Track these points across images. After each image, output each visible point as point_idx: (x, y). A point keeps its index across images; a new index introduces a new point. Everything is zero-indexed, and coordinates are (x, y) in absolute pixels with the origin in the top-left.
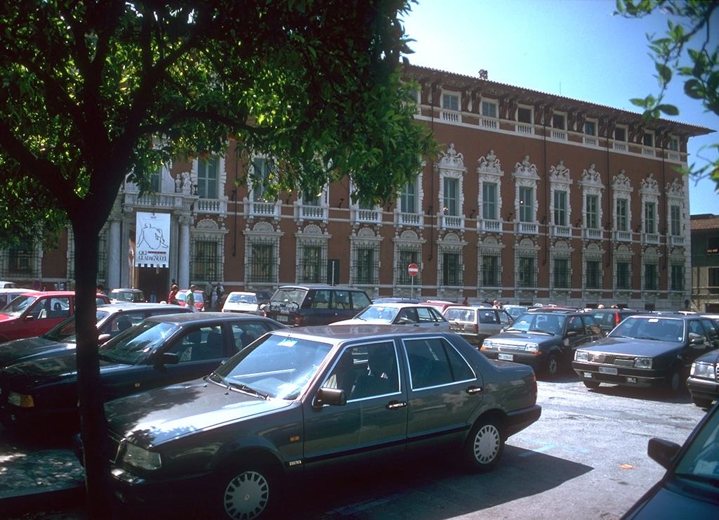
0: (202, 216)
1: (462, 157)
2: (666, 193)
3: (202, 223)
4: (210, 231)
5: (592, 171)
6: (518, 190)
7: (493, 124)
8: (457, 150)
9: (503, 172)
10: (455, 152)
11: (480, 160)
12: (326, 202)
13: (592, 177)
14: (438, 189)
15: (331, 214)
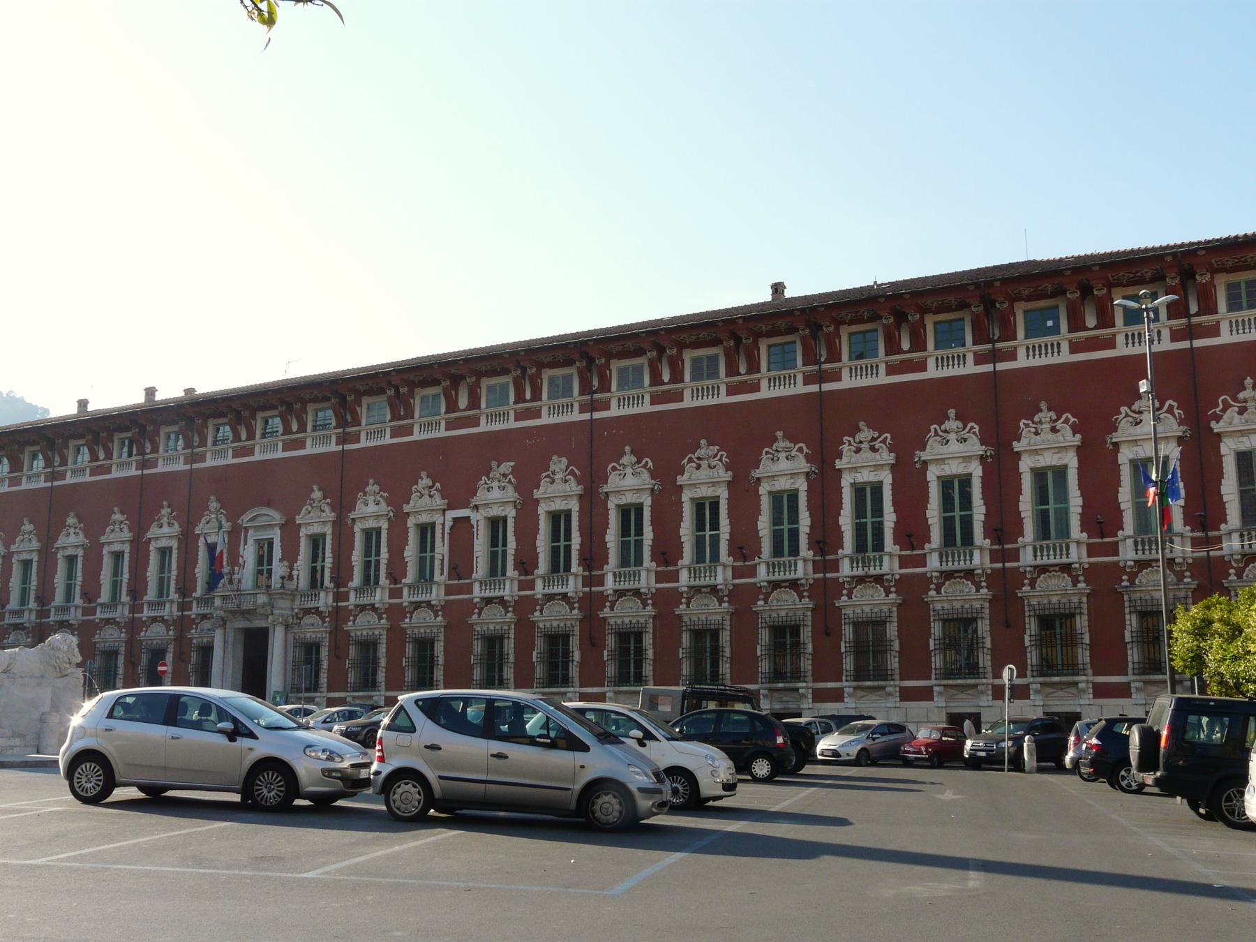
0: (307, 611)
1: (650, 464)
2: (1213, 424)
3: (308, 620)
4: (315, 629)
5: (952, 424)
6: (1027, 482)
7: (715, 390)
8: (962, 418)
9: (730, 473)
10: (634, 459)
11: (685, 461)
12: (442, 574)
13: (952, 437)
14: (606, 525)
15: (449, 590)
